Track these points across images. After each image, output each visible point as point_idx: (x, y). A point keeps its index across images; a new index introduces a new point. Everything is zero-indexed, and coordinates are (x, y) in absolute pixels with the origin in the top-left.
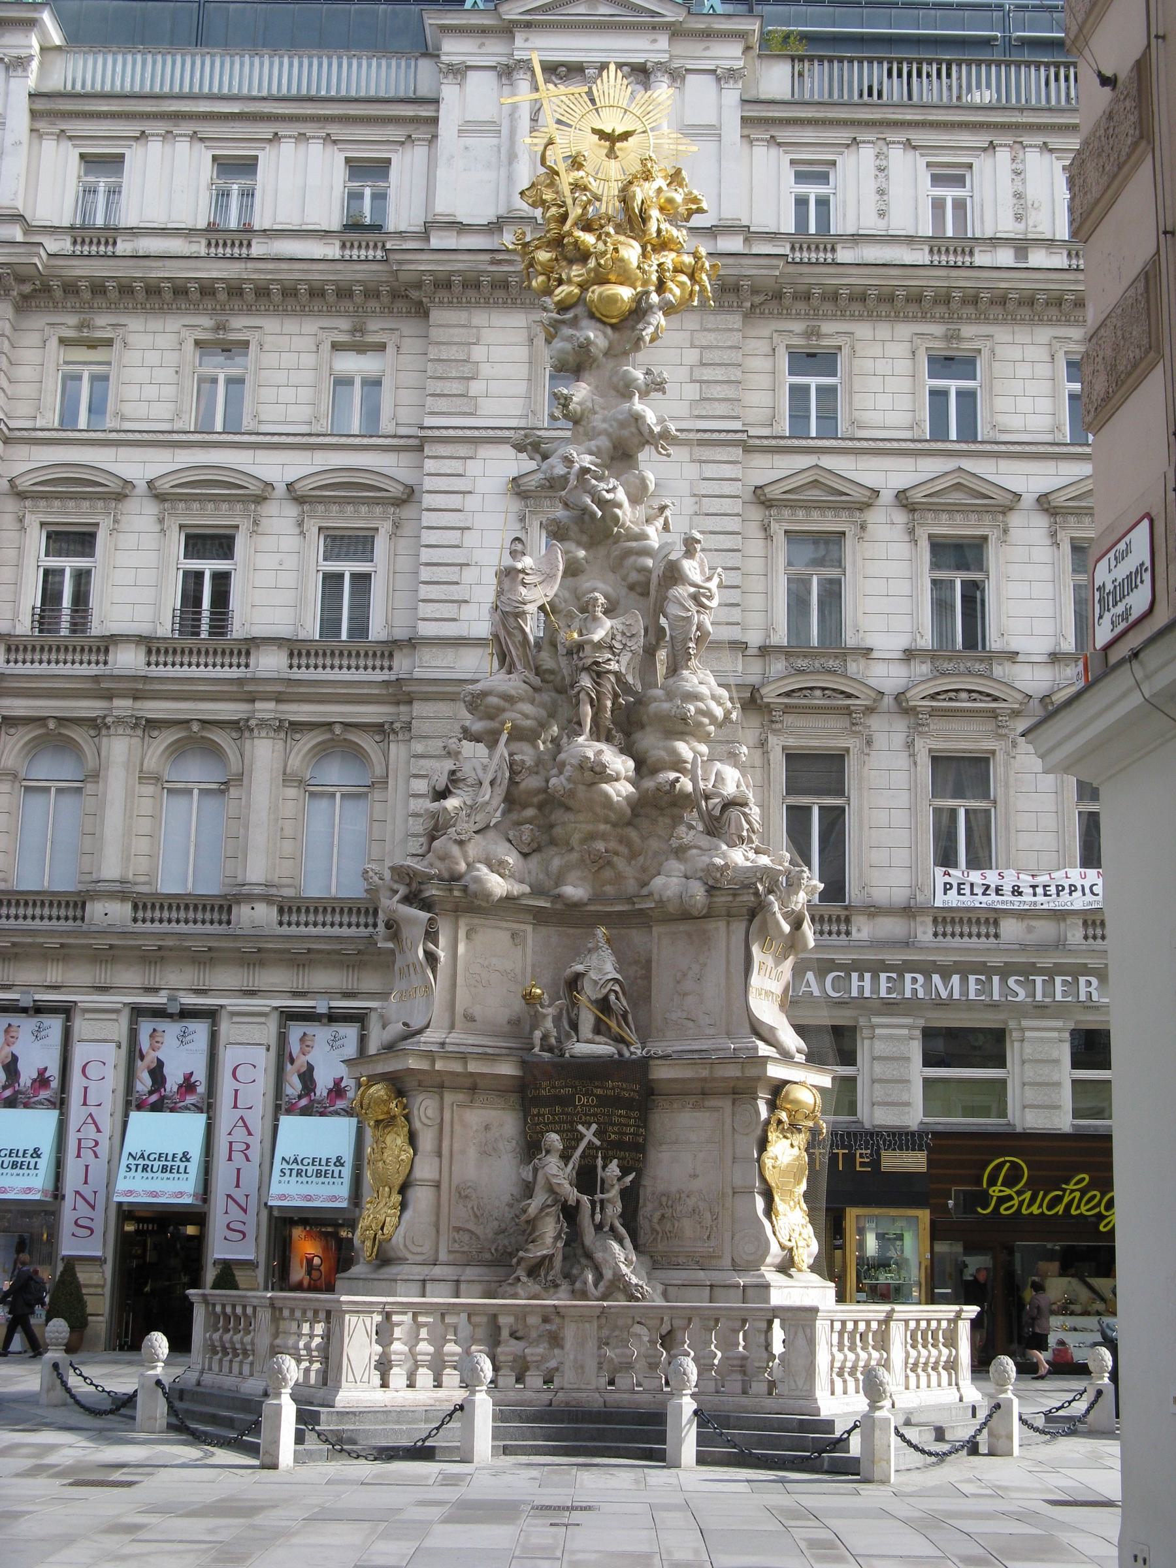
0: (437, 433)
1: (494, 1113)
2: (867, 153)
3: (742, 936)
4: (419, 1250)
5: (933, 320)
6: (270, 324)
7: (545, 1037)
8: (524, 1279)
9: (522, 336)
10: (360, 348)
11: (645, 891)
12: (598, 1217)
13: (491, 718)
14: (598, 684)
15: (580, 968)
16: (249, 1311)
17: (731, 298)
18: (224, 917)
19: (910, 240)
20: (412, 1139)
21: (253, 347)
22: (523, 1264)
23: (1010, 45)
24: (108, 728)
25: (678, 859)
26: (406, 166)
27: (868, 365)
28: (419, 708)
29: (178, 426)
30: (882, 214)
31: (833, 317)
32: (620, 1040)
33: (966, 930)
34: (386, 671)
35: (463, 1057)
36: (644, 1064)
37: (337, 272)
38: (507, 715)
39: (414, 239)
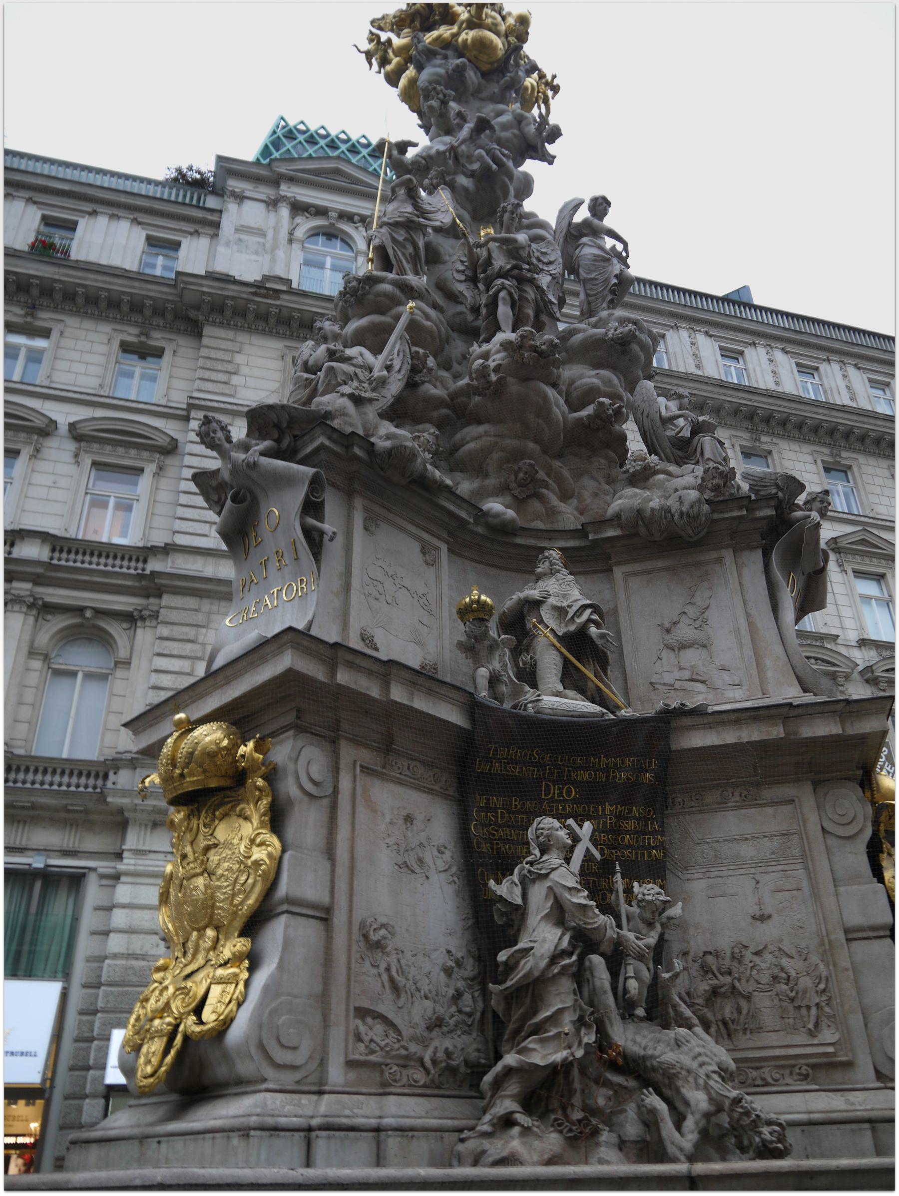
6: (72, 322)
8: (522, 1119)
13: (383, 313)
20: (276, 820)
21: (55, 334)
22: (513, 1088)
28: (166, 600)
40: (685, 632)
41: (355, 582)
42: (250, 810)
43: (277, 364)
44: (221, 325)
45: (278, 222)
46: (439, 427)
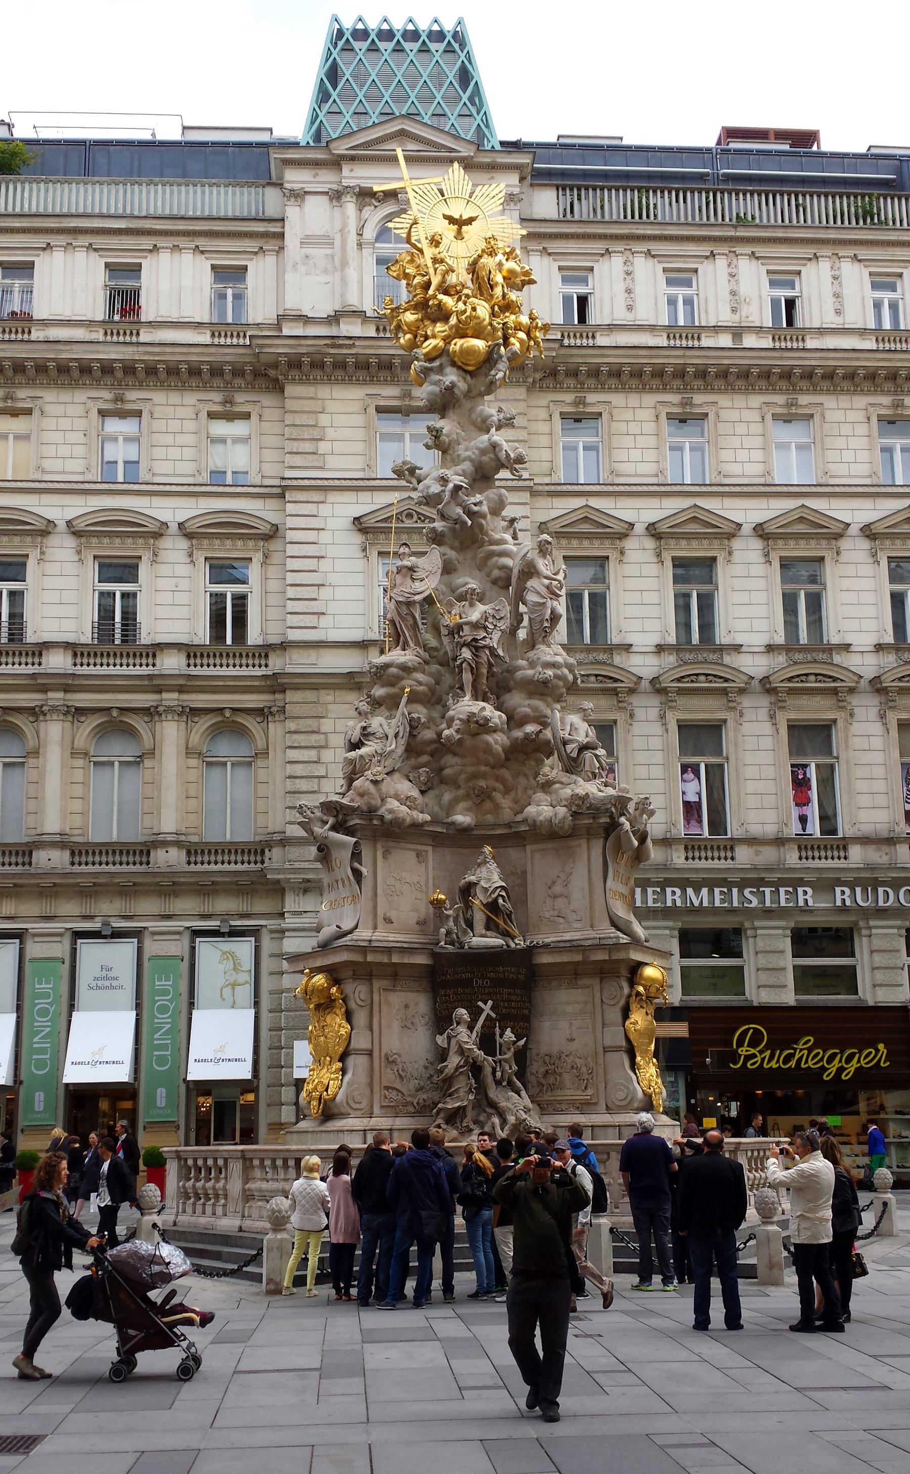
0: (295, 483)
1: (410, 995)
2: (617, 261)
3: (600, 851)
4: (358, 1106)
5: (672, 390)
6: (158, 397)
7: (448, 933)
9: (357, 407)
10: (230, 417)
11: (519, 818)
12: (499, 1074)
13: (392, 685)
14: (477, 656)
15: (473, 878)
16: (220, 1162)
17: (518, 375)
18: (144, 859)
19: (652, 329)
21: (145, 415)
22: (442, 1115)
23: (718, 179)
24: (45, 715)
25: (546, 792)
26: (260, 272)
27: (623, 427)
29: (89, 477)
30: (630, 308)
31: (595, 390)
32: (506, 934)
33: (709, 854)
34: (263, 668)
35: (389, 951)
36: (530, 951)
37: (211, 354)
38: (404, 682)
39: (269, 329)
40: (558, 889)
41: (379, 891)
42: (338, 1011)
43: (359, 420)
44: (301, 382)
45: (345, 218)
46: (432, 755)
